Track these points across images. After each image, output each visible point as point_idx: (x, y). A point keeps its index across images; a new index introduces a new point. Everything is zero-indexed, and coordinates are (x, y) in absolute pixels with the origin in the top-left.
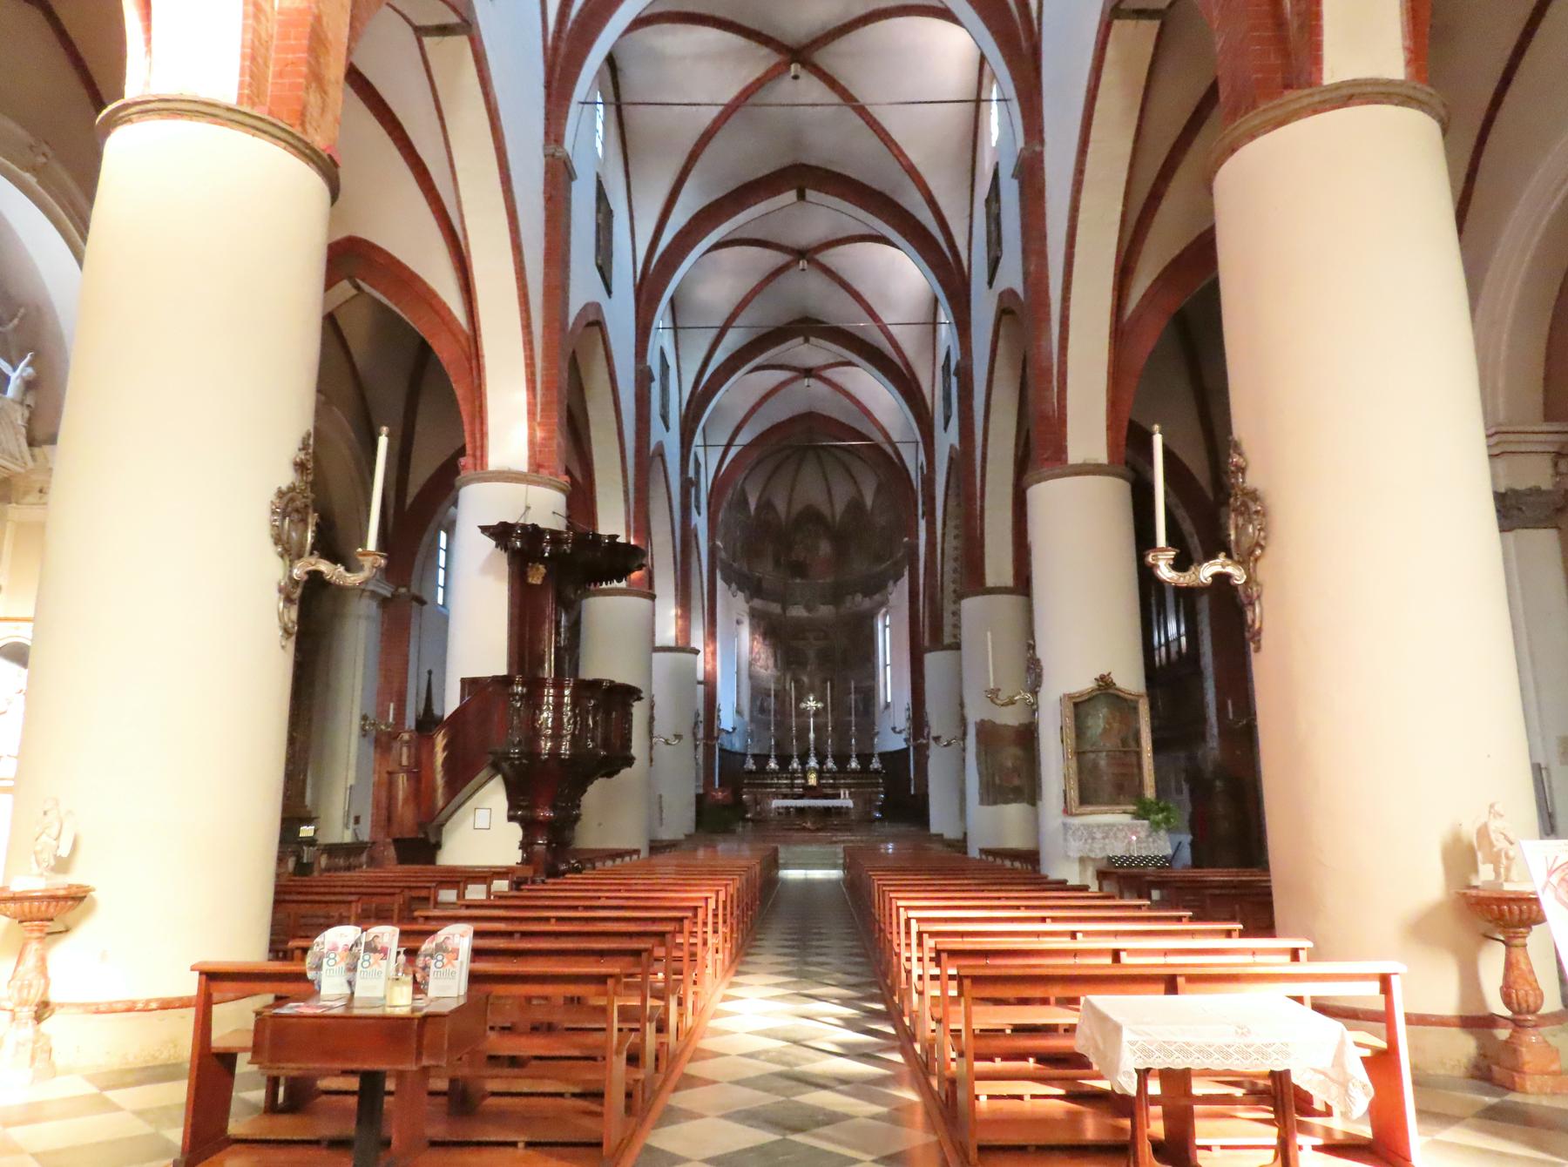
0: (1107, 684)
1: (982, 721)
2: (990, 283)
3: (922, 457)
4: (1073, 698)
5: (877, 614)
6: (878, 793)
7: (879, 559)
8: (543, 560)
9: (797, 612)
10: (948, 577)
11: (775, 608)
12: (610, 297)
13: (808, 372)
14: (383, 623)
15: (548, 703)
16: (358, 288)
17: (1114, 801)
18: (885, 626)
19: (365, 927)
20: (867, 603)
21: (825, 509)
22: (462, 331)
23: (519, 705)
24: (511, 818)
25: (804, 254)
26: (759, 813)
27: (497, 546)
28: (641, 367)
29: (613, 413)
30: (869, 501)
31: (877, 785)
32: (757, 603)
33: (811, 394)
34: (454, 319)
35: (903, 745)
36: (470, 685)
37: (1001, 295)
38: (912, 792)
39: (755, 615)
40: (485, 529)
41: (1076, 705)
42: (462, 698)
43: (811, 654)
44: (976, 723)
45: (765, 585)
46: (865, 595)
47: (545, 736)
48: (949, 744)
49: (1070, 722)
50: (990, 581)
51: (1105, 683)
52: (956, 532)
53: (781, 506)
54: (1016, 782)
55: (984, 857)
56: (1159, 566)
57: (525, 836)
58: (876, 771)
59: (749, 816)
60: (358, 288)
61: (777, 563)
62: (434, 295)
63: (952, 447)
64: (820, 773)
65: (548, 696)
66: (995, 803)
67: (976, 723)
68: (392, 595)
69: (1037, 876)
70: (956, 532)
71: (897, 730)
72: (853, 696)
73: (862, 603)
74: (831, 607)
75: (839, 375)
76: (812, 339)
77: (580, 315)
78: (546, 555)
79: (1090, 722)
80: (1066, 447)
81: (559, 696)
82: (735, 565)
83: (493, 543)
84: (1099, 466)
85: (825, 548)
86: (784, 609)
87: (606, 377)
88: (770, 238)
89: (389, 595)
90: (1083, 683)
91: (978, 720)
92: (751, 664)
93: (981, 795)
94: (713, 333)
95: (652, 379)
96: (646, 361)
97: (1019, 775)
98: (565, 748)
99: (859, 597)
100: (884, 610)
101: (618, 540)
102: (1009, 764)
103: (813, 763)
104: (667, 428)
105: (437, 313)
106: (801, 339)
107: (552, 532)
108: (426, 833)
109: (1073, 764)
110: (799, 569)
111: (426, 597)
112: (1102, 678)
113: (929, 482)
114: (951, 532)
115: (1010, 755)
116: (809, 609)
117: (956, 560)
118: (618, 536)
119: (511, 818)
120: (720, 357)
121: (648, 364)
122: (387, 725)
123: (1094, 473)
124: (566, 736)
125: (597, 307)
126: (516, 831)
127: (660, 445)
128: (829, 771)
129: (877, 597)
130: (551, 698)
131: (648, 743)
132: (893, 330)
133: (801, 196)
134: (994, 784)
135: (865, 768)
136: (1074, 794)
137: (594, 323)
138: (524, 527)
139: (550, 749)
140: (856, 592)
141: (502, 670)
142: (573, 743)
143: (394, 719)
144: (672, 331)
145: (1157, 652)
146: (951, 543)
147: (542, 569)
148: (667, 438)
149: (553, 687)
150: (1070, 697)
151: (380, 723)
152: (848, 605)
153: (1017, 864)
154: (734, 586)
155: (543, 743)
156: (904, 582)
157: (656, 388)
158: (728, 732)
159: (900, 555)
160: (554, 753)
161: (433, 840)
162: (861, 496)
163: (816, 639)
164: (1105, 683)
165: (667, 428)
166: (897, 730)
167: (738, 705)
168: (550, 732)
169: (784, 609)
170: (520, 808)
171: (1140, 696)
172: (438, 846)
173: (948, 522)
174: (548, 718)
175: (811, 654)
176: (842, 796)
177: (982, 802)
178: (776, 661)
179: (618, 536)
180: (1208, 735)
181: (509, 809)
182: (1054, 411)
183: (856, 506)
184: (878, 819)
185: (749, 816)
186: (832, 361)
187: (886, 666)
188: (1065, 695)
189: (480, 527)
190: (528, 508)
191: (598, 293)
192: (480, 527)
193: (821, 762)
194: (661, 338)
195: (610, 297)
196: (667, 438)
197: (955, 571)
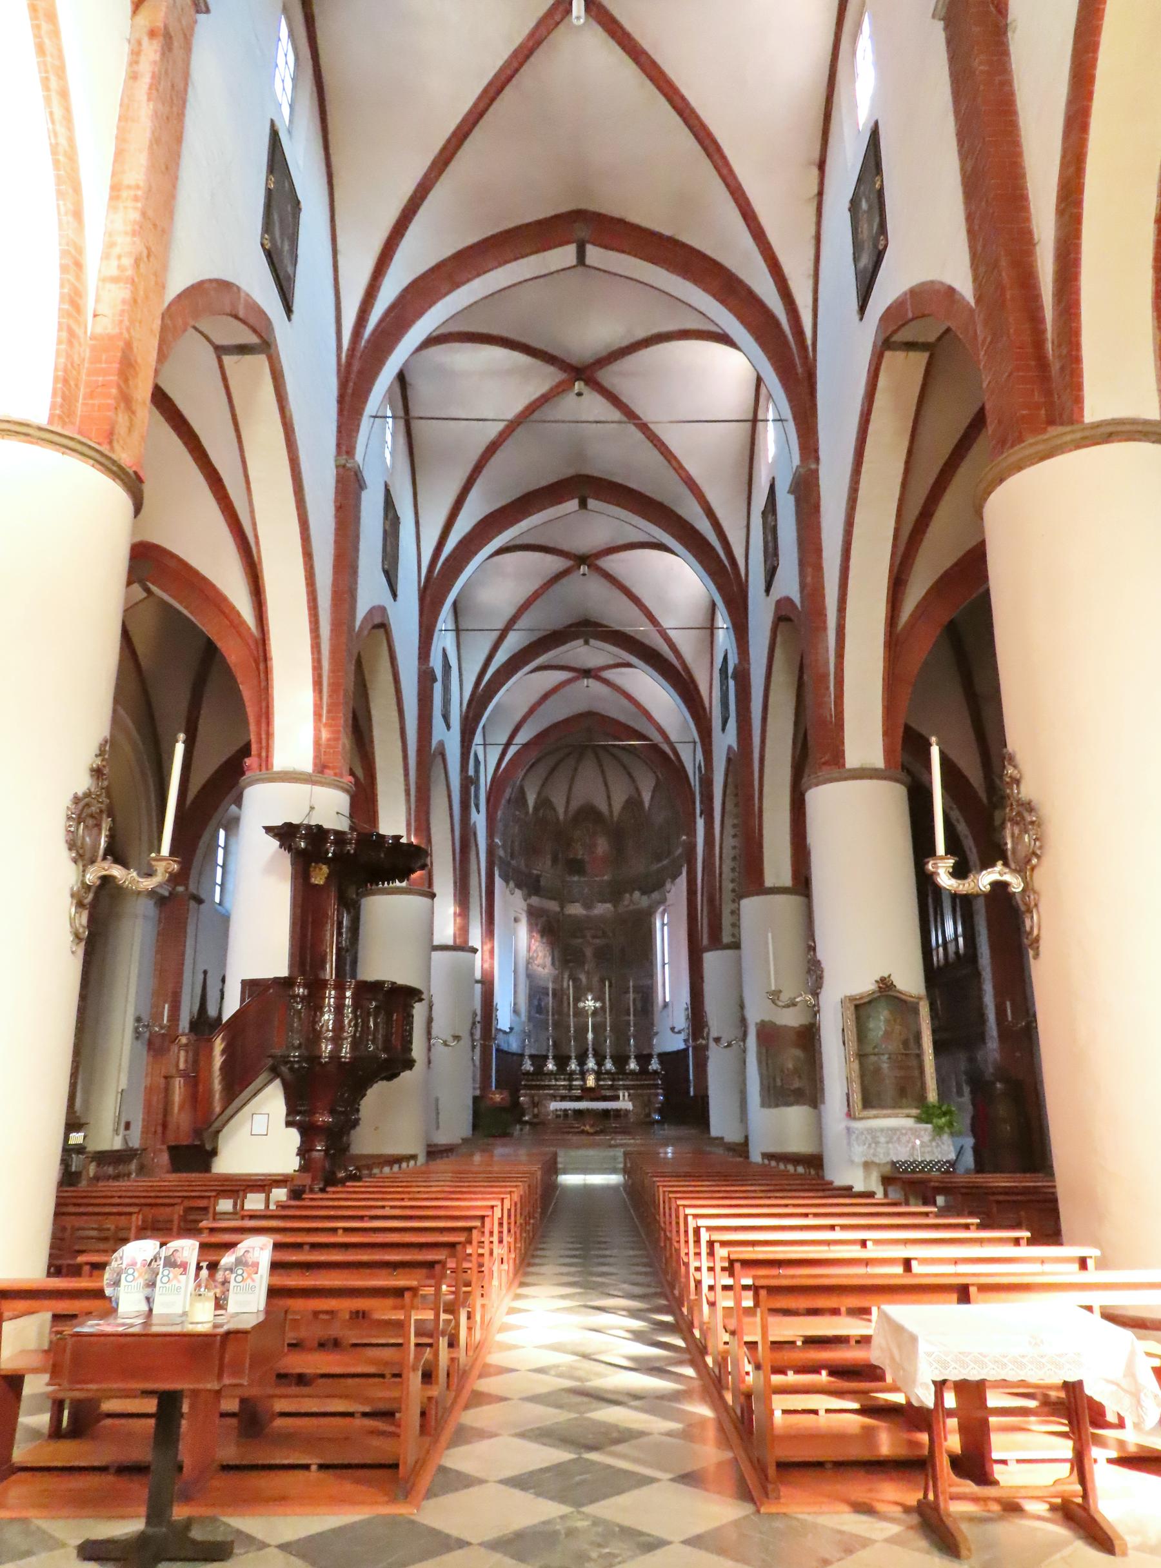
0: (887, 986)
1: (763, 1021)
2: (768, 590)
3: (700, 756)
4: (856, 999)
5: (655, 912)
6: (657, 1095)
8: (327, 861)
9: (576, 910)
11: (553, 906)
12: (395, 600)
13: (587, 673)
14: (160, 921)
15: (329, 1006)
16: (148, 590)
17: (896, 1105)
18: (663, 925)
19: (164, 1240)
20: (644, 901)
21: (603, 807)
22: (252, 634)
23: (300, 1007)
24: (289, 1124)
25: (585, 560)
26: (536, 1116)
27: (281, 846)
28: (424, 667)
29: (395, 714)
30: (647, 797)
31: (656, 1086)
32: (535, 900)
33: (587, 694)
34: (243, 623)
35: (682, 1046)
36: (251, 987)
37: (778, 602)
38: (692, 1094)
39: (534, 914)
40: (269, 830)
41: (857, 1007)
42: (242, 1000)
43: (589, 952)
44: (757, 1024)
45: (543, 883)
46: (644, 893)
47: (325, 1038)
48: (729, 1045)
49: (851, 1024)
51: (885, 986)
53: (559, 802)
54: (796, 1084)
55: (766, 1162)
56: (938, 874)
57: (302, 1142)
58: (655, 1072)
59: (527, 1118)
60: (148, 590)
61: (555, 860)
62: (225, 599)
63: (730, 748)
64: (599, 1075)
65: (330, 998)
66: (777, 1106)
67: (757, 1024)
68: (171, 893)
69: (822, 1182)
71: (676, 1030)
72: (631, 996)
73: (641, 900)
74: (609, 906)
75: (620, 677)
76: (592, 642)
77: (365, 619)
78: (330, 855)
79: (871, 1025)
80: (843, 751)
81: (340, 998)
82: (514, 862)
83: (278, 843)
84: (876, 770)
85: (602, 846)
86: (562, 907)
87: (390, 678)
88: (551, 545)
89: (166, 894)
90: (865, 985)
91: (758, 1021)
92: (528, 963)
94: (495, 635)
95: (435, 680)
96: (429, 661)
97: (800, 1077)
98: (346, 1051)
99: (637, 894)
100: (661, 909)
101: (402, 841)
102: (790, 1066)
103: (591, 1064)
104: (448, 727)
105: (227, 617)
106: (581, 642)
107: (337, 833)
108: (202, 1140)
109: (856, 1066)
110: (576, 867)
111: (203, 896)
112: (883, 980)
113: (707, 782)
114: (729, 831)
115: (791, 1057)
116: (588, 906)
117: (734, 859)
118: (401, 837)
119: (289, 1124)
120: (501, 658)
121: (431, 664)
122: (161, 1028)
123: (871, 778)
124: (346, 1039)
125: (382, 610)
126: (294, 1137)
127: (441, 744)
128: (608, 1072)
129: (655, 895)
130: (332, 1000)
131: (427, 1044)
132: (672, 634)
133: (583, 505)
134: (775, 1087)
135: (644, 1071)
136: (857, 1098)
137: (380, 625)
138: (309, 827)
139: (331, 1052)
140: (634, 890)
141: (283, 971)
142: (355, 1045)
143: (168, 1021)
144: (454, 633)
145: (934, 953)
146: (730, 842)
147: (325, 869)
148: (448, 737)
149: (335, 989)
150: (851, 999)
151: (154, 1025)
152: (626, 903)
153: (800, 1169)
154: (512, 884)
155: (323, 1046)
156: (682, 880)
157: (438, 687)
158: (505, 1032)
160: (335, 1056)
161: (208, 1147)
162: (639, 794)
163: (594, 937)
164: (885, 986)
165: (448, 727)
166: (676, 1030)
167: (515, 1004)
168: (331, 1034)
170: (299, 1113)
171: (920, 998)
172: (214, 1153)
173: (726, 822)
174: (329, 1020)
175: (589, 952)
176: (621, 1098)
177: (764, 1104)
178: (553, 959)
179: (401, 837)
180: (987, 1037)
181: (288, 1115)
182: (831, 715)
183: (634, 803)
184: (658, 1122)
185: (527, 1118)
186: (611, 662)
187: (664, 965)
188: (846, 997)
189: (264, 827)
190: (312, 808)
191: (384, 598)
192: (264, 827)
193: (600, 1062)
194: (444, 640)
195: (395, 600)
196: (448, 737)
197: (733, 870)
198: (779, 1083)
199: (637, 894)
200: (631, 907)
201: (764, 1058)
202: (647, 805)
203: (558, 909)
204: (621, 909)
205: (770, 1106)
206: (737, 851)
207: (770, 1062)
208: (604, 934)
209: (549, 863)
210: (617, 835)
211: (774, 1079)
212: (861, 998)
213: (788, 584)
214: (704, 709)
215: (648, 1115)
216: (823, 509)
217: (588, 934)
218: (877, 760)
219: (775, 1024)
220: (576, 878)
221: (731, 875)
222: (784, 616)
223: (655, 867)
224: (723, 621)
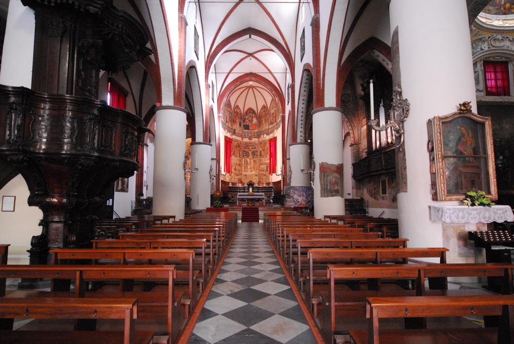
4: (442, 119)
7: (272, 123)
9: (246, 140)
10: (300, 118)
13: (250, 55)
21: (255, 109)
31: (271, 191)
33: (249, 66)
35: (280, 179)
43: (250, 153)
44: (320, 164)
45: (236, 131)
50: (327, 105)
52: (303, 102)
54: (336, 188)
61: (240, 125)
66: (327, 196)
67: (320, 164)
70: (303, 102)
74: (257, 139)
75: (263, 56)
82: (227, 124)
85: (255, 121)
86: (242, 139)
91: (321, 162)
93: (321, 193)
94: (226, 75)
99: (265, 135)
102: (334, 181)
106: (248, 36)
110: (247, 127)
112: (464, 104)
114: (301, 102)
115: (333, 177)
116: (250, 138)
117: (302, 112)
120: (219, 40)
131: (184, 172)
132: (276, 75)
133: (250, 37)
134: (327, 188)
146: (301, 106)
152: (262, 138)
154: (226, 130)
156: (280, 129)
159: (278, 121)
162: (266, 104)
169: (242, 139)
173: (300, 98)
175: (250, 153)
183: (264, 107)
197: (302, 116)
198: (329, 188)
199: (265, 135)
200: (264, 139)
201: (323, 177)
202: (269, 106)
203: (241, 140)
204: (260, 140)
205: (406, 189)
206: (304, 109)
207: (325, 179)
208: (255, 148)
209: (238, 125)
210: (259, 118)
211: (327, 185)
212: (446, 118)
213: (309, 58)
214: (292, 60)
215: (269, 200)
216: (321, 29)
217: (250, 147)
218: (334, 105)
219: (328, 164)
220: (247, 131)
221: (301, 122)
222: (307, 70)
223: (271, 126)
224: (289, 71)
